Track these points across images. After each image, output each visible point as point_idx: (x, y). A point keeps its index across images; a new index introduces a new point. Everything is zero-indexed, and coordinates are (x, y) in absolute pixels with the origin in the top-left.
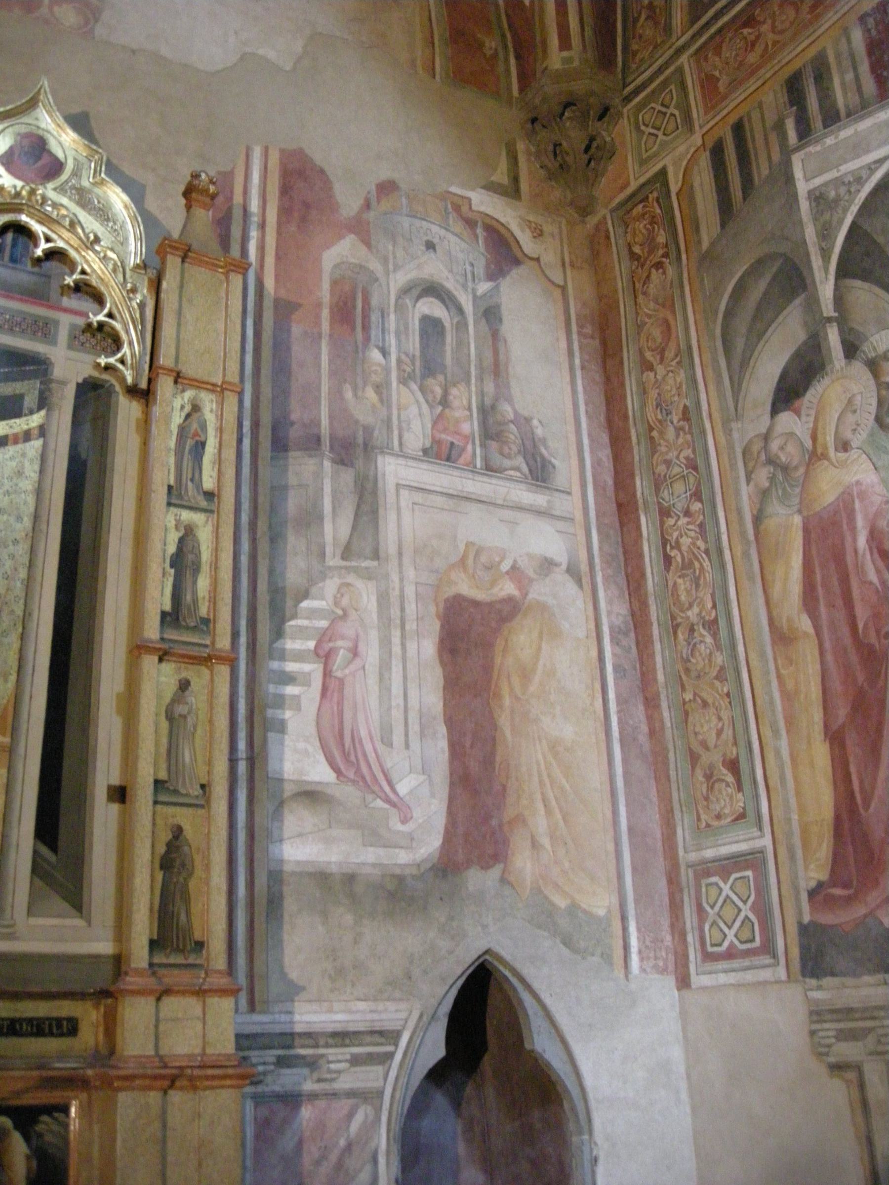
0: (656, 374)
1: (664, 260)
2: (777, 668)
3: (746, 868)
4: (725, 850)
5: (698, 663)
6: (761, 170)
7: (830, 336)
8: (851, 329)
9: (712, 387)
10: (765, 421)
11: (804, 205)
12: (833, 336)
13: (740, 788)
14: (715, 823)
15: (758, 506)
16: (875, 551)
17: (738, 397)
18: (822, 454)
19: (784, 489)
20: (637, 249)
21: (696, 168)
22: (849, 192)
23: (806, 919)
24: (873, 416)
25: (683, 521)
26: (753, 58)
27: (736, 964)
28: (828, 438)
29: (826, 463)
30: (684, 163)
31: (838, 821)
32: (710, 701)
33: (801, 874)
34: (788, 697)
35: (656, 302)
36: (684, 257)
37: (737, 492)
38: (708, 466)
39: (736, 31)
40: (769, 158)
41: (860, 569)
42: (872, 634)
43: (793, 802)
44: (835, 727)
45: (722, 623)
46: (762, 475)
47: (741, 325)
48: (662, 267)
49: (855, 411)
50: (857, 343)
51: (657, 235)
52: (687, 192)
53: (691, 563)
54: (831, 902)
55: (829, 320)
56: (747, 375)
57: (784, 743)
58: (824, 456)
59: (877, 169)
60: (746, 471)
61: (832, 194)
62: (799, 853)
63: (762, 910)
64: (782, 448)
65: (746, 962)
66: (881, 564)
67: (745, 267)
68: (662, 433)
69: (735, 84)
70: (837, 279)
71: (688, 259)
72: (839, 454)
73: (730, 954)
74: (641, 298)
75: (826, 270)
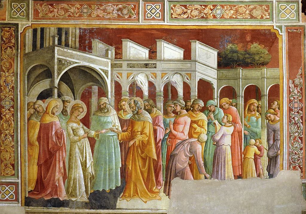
0: (5, 74)
1: (13, 47)
2: (28, 150)
3: (14, 185)
4: (7, 181)
5: (6, 142)
6: (46, 44)
9: (22, 86)
10: (35, 100)
11: (56, 61)
12: (56, 91)
13: (14, 170)
14: (6, 175)
16: (56, 136)
20: (4, 39)
21: (27, 31)
22: (68, 65)
23: (27, 196)
25: (7, 111)
26: (51, 15)
27: (8, 202)
30: (24, 27)
31: (37, 180)
32: (9, 151)
33: (27, 188)
34: (30, 156)
35: (8, 56)
36: (19, 50)
37: (24, 111)
38: (17, 102)
39: (47, 4)
40: (49, 43)
41: (52, 138)
42: (52, 150)
43: (27, 175)
45: (15, 136)
46: (32, 111)
47: (33, 77)
52: (24, 34)
53: (8, 121)
54: (33, 194)
55: (56, 87)
57: (27, 164)
60: (27, 109)
61: (63, 62)
62: (27, 184)
63: (16, 193)
65: (11, 202)
68: (4, 89)
69: (43, 18)
70: (60, 80)
73: (7, 200)
74: (3, 52)
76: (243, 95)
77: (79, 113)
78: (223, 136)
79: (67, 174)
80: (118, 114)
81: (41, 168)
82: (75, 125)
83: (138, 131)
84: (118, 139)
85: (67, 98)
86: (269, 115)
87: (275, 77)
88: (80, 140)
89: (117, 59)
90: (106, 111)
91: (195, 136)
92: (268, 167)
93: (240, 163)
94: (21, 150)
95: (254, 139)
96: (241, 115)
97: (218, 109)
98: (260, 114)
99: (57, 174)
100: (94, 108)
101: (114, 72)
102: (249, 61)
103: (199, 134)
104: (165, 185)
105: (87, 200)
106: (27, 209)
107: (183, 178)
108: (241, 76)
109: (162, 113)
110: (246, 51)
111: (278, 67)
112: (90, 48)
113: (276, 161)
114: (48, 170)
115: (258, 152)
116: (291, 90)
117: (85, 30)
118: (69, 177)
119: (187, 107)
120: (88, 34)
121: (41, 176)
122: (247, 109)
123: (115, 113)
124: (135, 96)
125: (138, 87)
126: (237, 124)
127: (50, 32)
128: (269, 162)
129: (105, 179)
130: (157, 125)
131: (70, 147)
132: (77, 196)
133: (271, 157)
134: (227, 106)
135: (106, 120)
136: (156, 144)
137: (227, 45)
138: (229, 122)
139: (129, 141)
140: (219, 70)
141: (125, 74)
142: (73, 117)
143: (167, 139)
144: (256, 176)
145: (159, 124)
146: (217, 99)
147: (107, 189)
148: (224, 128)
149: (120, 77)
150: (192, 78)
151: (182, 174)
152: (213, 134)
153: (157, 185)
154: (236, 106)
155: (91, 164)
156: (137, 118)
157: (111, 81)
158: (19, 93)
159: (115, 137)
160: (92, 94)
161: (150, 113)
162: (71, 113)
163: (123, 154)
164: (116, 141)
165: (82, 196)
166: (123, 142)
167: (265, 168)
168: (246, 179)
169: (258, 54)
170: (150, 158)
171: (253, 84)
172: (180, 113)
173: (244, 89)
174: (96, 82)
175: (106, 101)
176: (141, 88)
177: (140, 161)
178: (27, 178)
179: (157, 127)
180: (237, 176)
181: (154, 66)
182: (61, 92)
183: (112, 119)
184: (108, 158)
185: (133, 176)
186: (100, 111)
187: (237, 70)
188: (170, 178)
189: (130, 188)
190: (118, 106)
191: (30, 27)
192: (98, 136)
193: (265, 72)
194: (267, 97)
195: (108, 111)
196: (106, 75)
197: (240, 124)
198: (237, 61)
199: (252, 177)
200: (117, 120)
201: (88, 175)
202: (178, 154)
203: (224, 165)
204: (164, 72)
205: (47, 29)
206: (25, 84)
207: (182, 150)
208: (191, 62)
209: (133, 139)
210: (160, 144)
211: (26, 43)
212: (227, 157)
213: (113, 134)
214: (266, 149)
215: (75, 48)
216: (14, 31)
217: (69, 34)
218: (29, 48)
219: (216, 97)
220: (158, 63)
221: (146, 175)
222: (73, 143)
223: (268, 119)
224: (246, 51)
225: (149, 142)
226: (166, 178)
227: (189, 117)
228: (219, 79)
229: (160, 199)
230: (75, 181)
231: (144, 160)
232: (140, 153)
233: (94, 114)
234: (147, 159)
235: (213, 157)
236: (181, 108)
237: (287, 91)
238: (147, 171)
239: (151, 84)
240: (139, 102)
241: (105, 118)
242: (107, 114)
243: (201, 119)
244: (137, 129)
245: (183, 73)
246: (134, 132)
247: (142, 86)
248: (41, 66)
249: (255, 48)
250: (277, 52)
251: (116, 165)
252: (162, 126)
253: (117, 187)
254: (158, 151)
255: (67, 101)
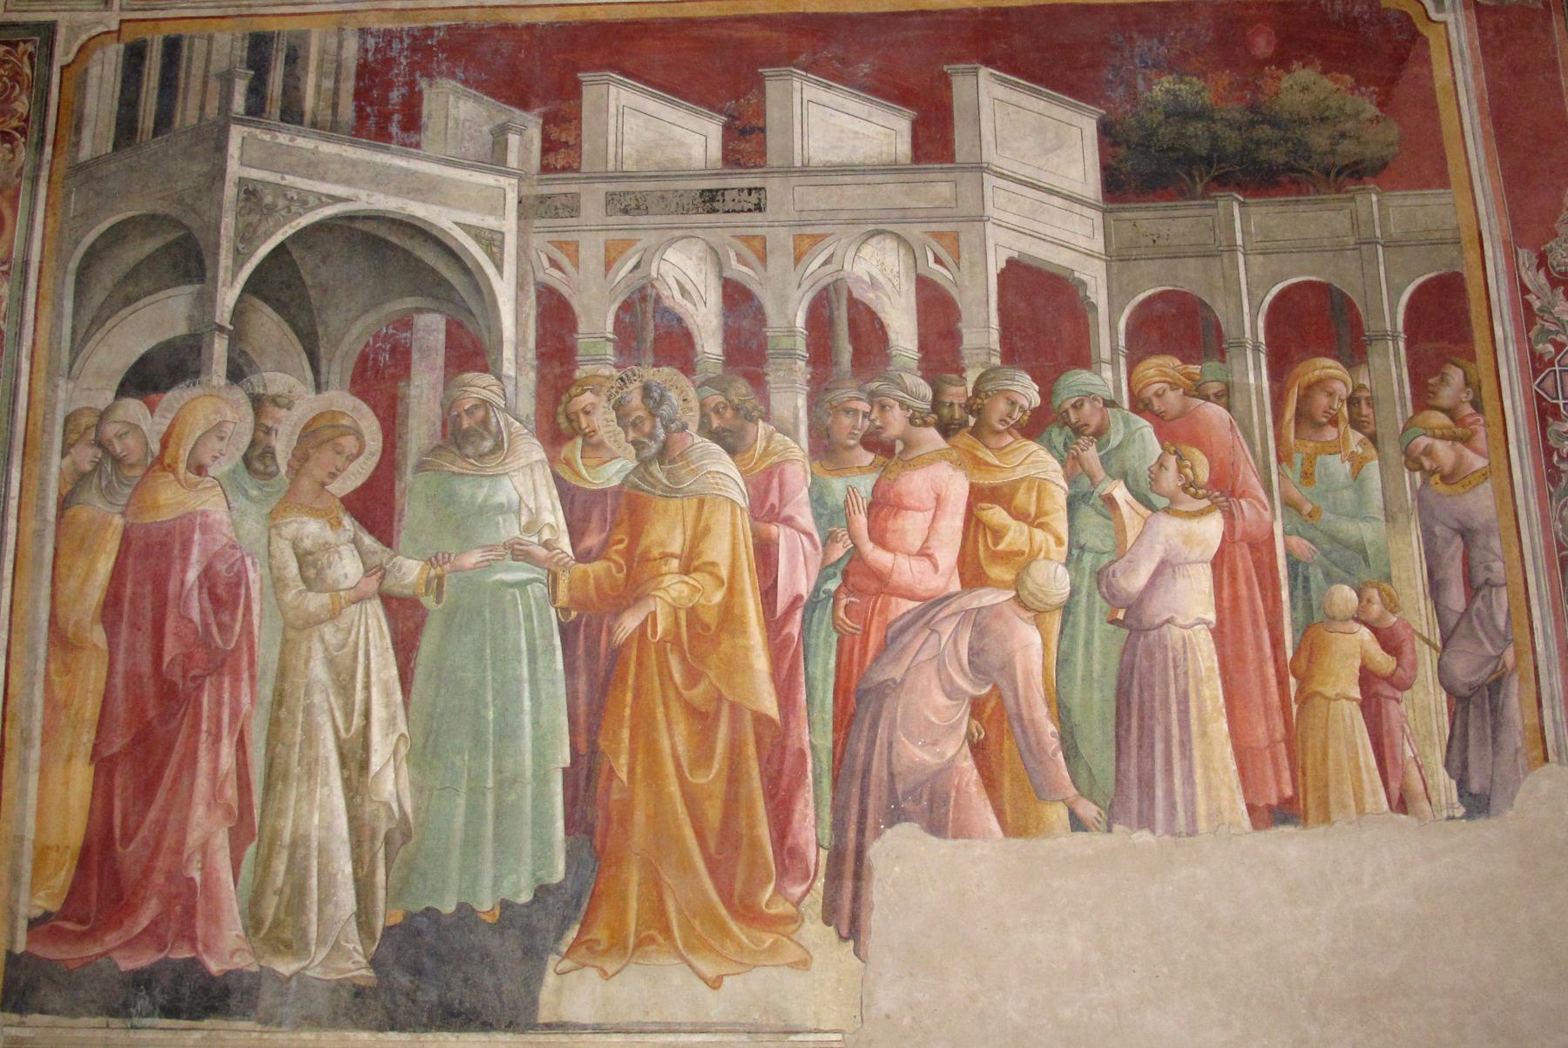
1: (18, 135)
2: (47, 674)
6: (187, 114)
7: (216, 346)
8: (243, 353)
9: (44, 324)
10: (106, 397)
11: (230, 192)
12: (220, 347)
15: (69, 487)
16: (205, 590)
17: (77, 354)
18: (169, 466)
19: (110, 482)
21: (98, 55)
22: (289, 211)
23: (20, 948)
24: (242, 454)
28: (181, 452)
29: (172, 477)
30: (84, 38)
31: (86, 850)
33: (24, 897)
34: (53, 706)
36: (48, 149)
37: (46, 460)
40: (202, 108)
41: (183, 600)
42: (178, 671)
44: (106, 754)
46: (86, 456)
47: (107, 277)
48: (11, 143)
49: (222, 439)
50: (245, 369)
51: (16, 99)
52: (76, 72)
54: (57, 935)
55: (221, 329)
56: (98, 336)
57: (35, 754)
58: (172, 469)
59: (328, 204)
60: (64, 443)
62: (26, 877)
64: (119, 437)
66: (207, 605)
67: (131, 214)
70: (244, 290)
71: (53, 155)
72: (190, 475)
75: (235, 276)
76: (1262, 338)
77: (340, 464)
78: (1165, 568)
79: (257, 812)
80: (552, 461)
81: (110, 775)
82: (312, 529)
83: (666, 556)
84: (554, 600)
85: (276, 381)
86: (1423, 441)
87: (1437, 235)
88: (334, 614)
89: (555, 170)
90: (488, 444)
91: (996, 572)
92: (1455, 751)
93: (1280, 731)
94: (14, 678)
95: (1352, 587)
96: (1258, 448)
97: (1127, 422)
98: (1373, 439)
99: (199, 811)
100: (420, 430)
101: (537, 241)
102: (1278, 156)
103: (1021, 561)
104: (834, 875)
105: (365, 974)
106: (13, 1031)
107: (937, 828)
108: (1239, 236)
109: (807, 450)
110: (1253, 108)
111: (1445, 184)
112: (412, 122)
113: (1496, 711)
114: (146, 790)
115: (1383, 662)
116: (1536, 304)
117: (389, 36)
118: (268, 830)
119: (945, 412)
120: (407, 57)
121: (110, 829)
122: (1290, 413)
123: (538, 453)
124: (650, 358)
125: (667, 310)
126: (1243, 502)
127: (209, 53)
128: (1458, 722)
129: (472, 843)
130: (774, 516)
131: (282, 653)
132: (306, 947)
133: (1464, 691)
134: (1173, 399)
135: (488, 496)
136: (774, 625)
137: (1149, 83)
138: (1192, 490)
139: (617, 614)
140: (1112, 211)
141: (591, 249)
142: (306, 484)
143: (835, 596)
144: (1385, 806)
145: (788, 511)
146: (1114, 363)
147: (486, 904)
148: (1169, 527)
149: (564, 261)
150: (965, 255)
151: (931, 802)
152: (1105, 560)
153: (783, 871)
154: (1225, 396)
155: (395, 753)
156: (659, 481)
157: (520, 286)
158: (25, 366)
159: (539, 590)
160: (415, 356)
161: (732, 451)
162: (296, 464)
163: (582, 684)
164: (540, 614)
165: (337, 946)
166: (579, 616)
167: (1436, 758)
168: (1322, 829)
169: (1323, 120)
170: (734, 707)
171: (1313, 278)
172: (908, 445)
173: (1265, 305)
174: (432, 287)
175: (486, 394)
176: (680, 320)
177: (681, 728)
178: (30, 834)
179: (773, 529)
180: (1269, 807)
181: (754, 198)
182: (248, 350)
183: (521, 489)
184: (491, 715)
185: (639, 816)
186: (454, 449)
187: (1215, 206)
188: (861, 831)
189: (623, 897)
190: (555, 415)
191: (115, 35)
192: (440, 586)
193: (1376, 216)
194: (1402, 345)
195: (498, 446)
196: (491, 256)
197: (1261, 502)
198: (1208, 161)
199: (1361, 811)
200: (550, 494)
201: (377, 817)
202: (903, 680)
203: (1185, 744)
204: (809, 230)
205: (197, 40)
206: (60, 316)
207: (922, 657)
208: (958, 174)
209: (637, 600)
210: (794, 628)
211: (87, 111)
212: (1198, 693)
213: (523, 576)
214: (1428, 641)
215: (329, 128)
216: (31, 57)
217: (307, 58)
218: (96, 138)
219: (1105, 353)
220: (774, 185)
221: (713, 813)
222: (297, 628)
223: (1421, 468)
224: (1253, 108)
225: (729, 615)
226: (839, 826)
227: (958, 465)
228: (1118, 257)
229: (803, 964)
230: (301, 852)
231: (702, 718)
232: (677, 676)
233: (421, 467)
234: (718, 712)
235: (1110, 693)
236: (911, 421)
237: (1513, 301)
238: (720, 789)
239: (736, 297)
240: (673, 395)
241: (481, 486)
242: (491, 466)
243: (1030, 480)
244: (662, 544)
245: (915, 232)
246: (646, 558)
247: (690, 307)
248: (149, 223)
249: (1305, 89)
250: (1429, 105)
251: (540, 755)
252: (806, 519)
253: (542, 891)
254: (786, 665)
255: (275, 401)
